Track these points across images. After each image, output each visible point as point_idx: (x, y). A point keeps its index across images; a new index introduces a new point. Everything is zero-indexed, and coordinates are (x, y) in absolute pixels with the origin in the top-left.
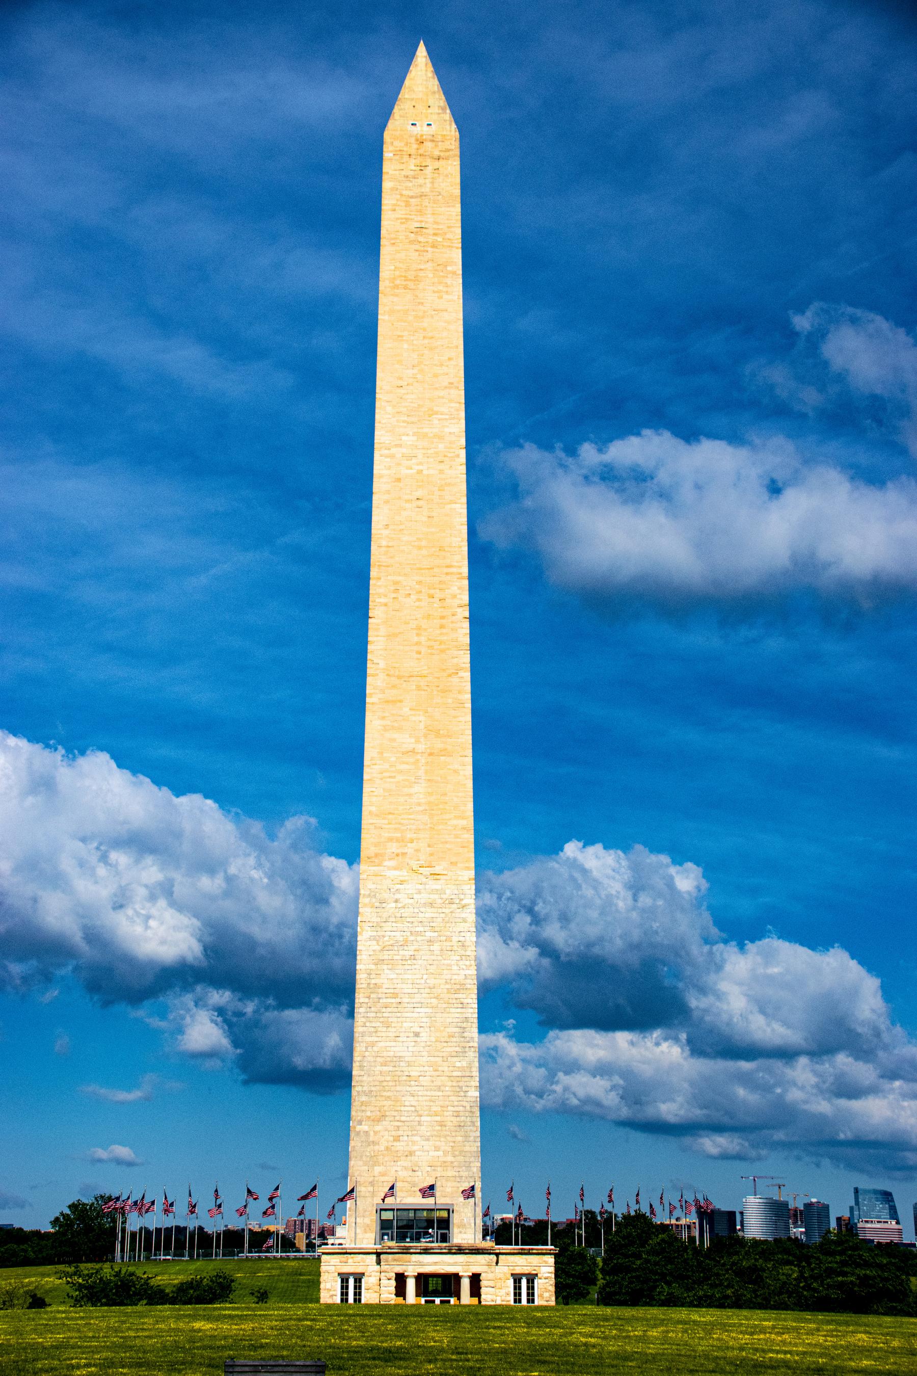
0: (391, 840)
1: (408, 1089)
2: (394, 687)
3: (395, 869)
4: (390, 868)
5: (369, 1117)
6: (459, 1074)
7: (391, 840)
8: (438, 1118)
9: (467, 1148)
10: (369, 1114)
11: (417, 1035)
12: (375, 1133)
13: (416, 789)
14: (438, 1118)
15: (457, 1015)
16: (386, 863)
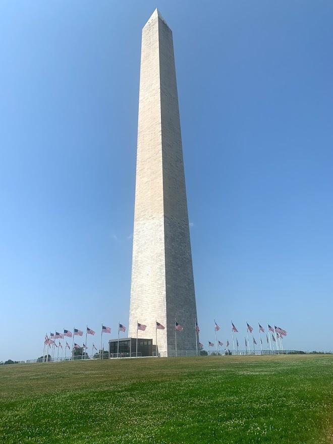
0: (142, 212)
1: (146, 295)
2: (143, 165)
3: (143, 220)
4: (141, 221)
5: (135, 308)
6: (159, 286)
7: (142, 212)
8: (153, 305)
9: (162, 315)
10: (134, 307)
11: (148, 275)
12: (136, 313)
13: (149, 193)
14: (153, 305)
15: (159, 265)
16: (140, 220)
